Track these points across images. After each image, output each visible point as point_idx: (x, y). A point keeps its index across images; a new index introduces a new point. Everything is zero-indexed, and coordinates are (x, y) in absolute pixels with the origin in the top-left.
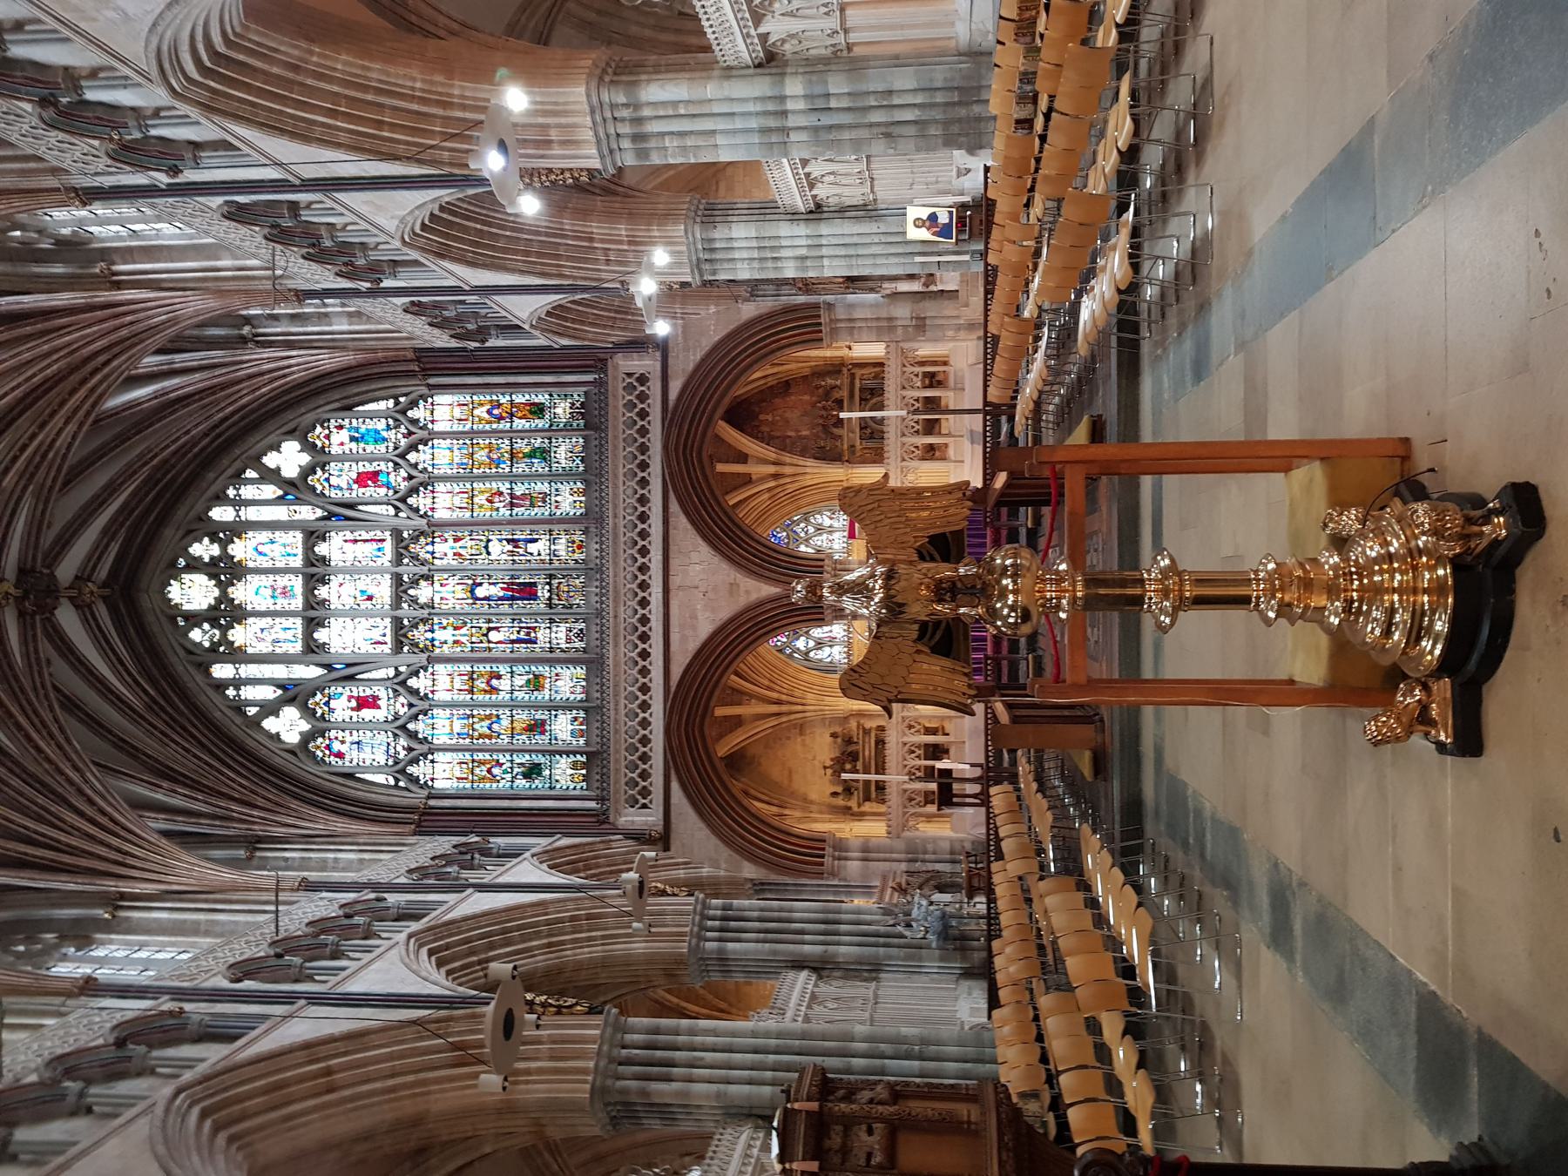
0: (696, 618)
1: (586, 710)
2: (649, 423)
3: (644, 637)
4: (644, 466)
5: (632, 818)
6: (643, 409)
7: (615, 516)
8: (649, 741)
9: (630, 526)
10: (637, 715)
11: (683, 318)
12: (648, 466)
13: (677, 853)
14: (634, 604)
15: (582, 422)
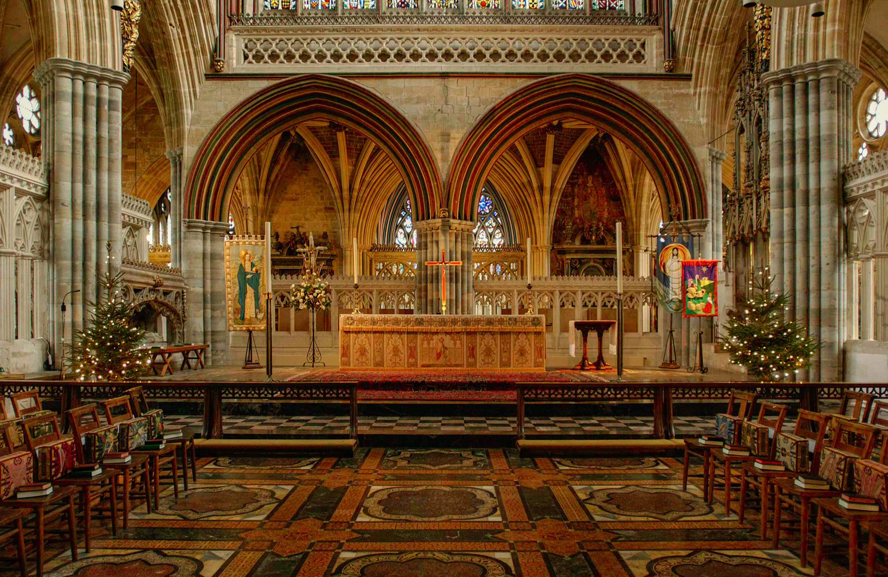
0: (417, 103)
1: (335, 9)
2: (599, 62)
3: (400, 56)
4: (559, 57)
5: (235, 45)
6: (611, 56)
7: (512, 30)
8: (305, 61)
9: (503, 44)
10: (328, 50)
11: (695, 93)
12: (559, 60)
13: (205, 87)
14: (431, 46)
15: (596, 7)
